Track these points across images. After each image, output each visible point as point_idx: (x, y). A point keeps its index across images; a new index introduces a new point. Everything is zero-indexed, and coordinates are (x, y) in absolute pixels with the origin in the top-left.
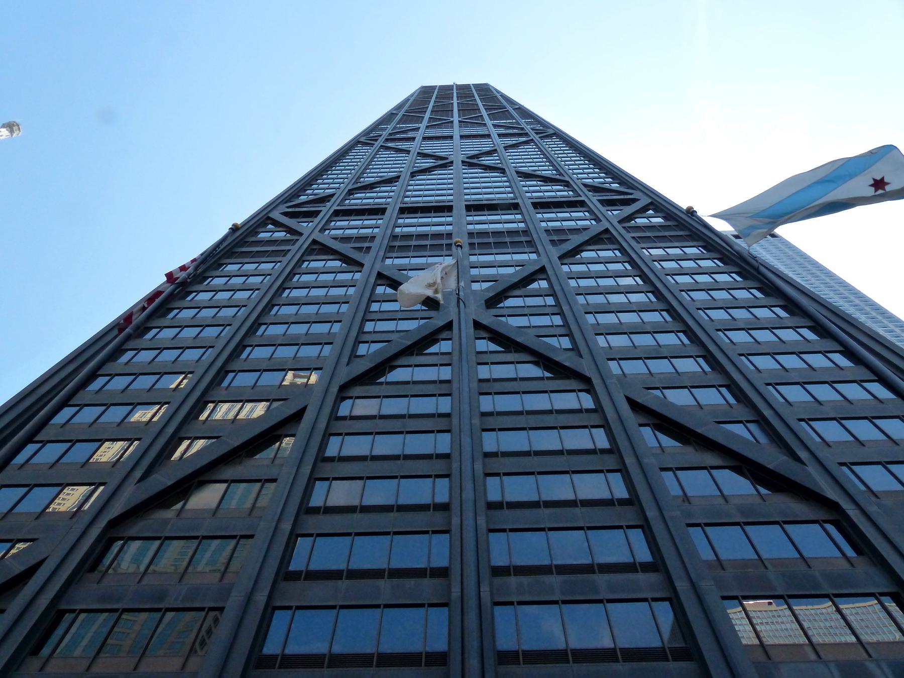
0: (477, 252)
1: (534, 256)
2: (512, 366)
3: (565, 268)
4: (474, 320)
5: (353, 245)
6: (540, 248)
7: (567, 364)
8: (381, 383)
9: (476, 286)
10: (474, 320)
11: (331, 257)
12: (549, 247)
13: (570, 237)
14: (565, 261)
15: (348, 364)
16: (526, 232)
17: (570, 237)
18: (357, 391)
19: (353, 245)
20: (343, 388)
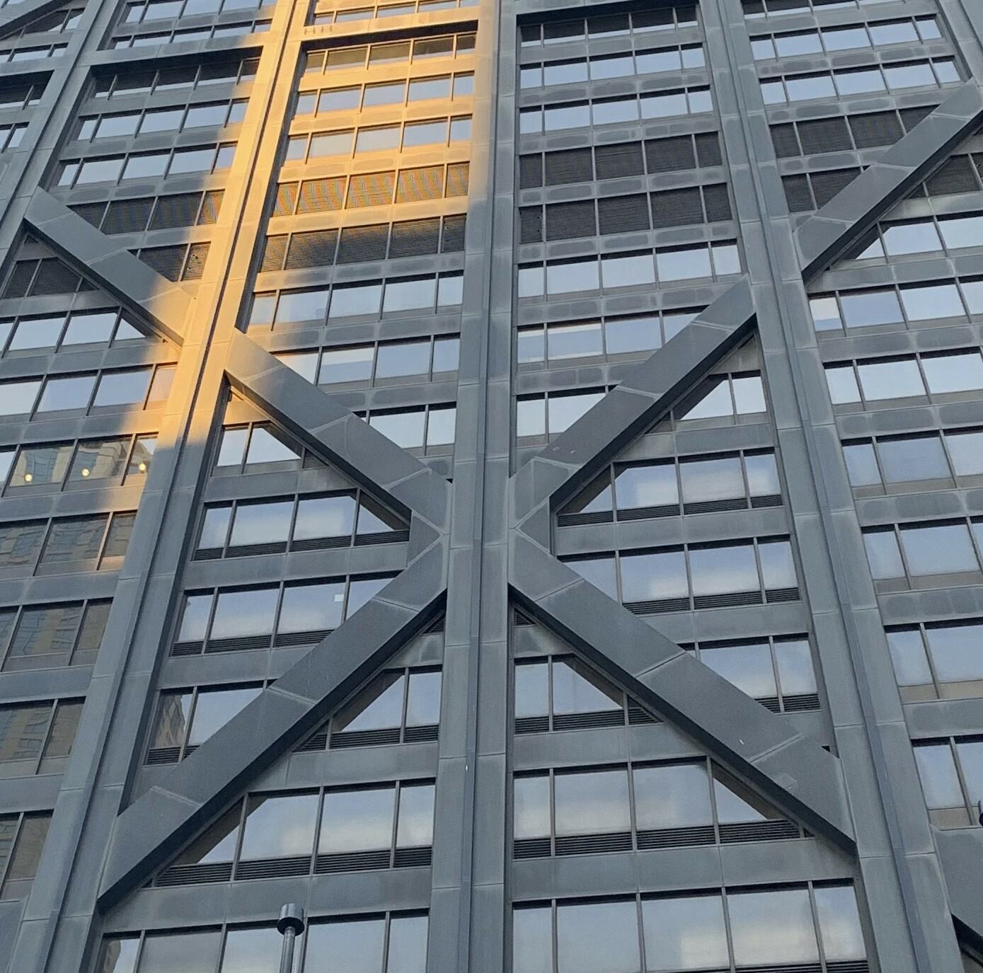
0: (544, 250)
1: (727, 260)
2: (621, 774)
3: (824, 311)
4: (511, 588)
5: (143, 239)
6: (748, 226)
7: (784, 781)
8: (221, 872)
9: (532, 419)
10: (511, 588)
11: (79, 300)
12: (784, 220)
13: (858, 157)
14: (829, 281)
15: (122, 809)
16: (707, 143)
17: (858, 157)
18: (151, 905)
19: (143, 239)
20: (109, 903)
